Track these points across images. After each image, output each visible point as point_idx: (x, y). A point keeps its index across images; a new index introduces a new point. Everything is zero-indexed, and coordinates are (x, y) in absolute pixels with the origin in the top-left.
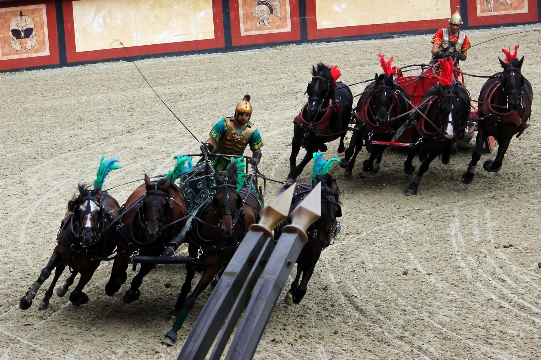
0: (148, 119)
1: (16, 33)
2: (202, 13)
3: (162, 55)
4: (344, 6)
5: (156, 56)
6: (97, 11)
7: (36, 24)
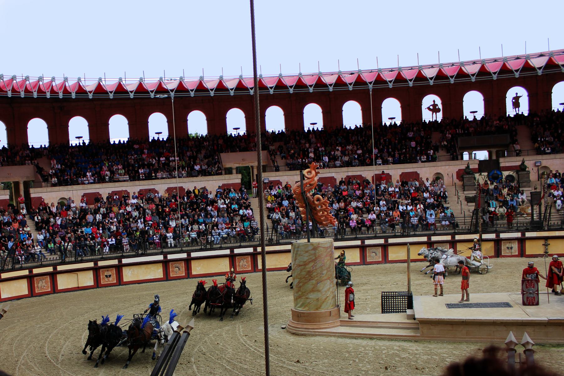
0: (144, 300)
1: (106, 276)
2: (160, 270)
3: (148, 282)
4: (200, 268)
5: (147, 283)
6: (130, 270)
7: (112, 273)
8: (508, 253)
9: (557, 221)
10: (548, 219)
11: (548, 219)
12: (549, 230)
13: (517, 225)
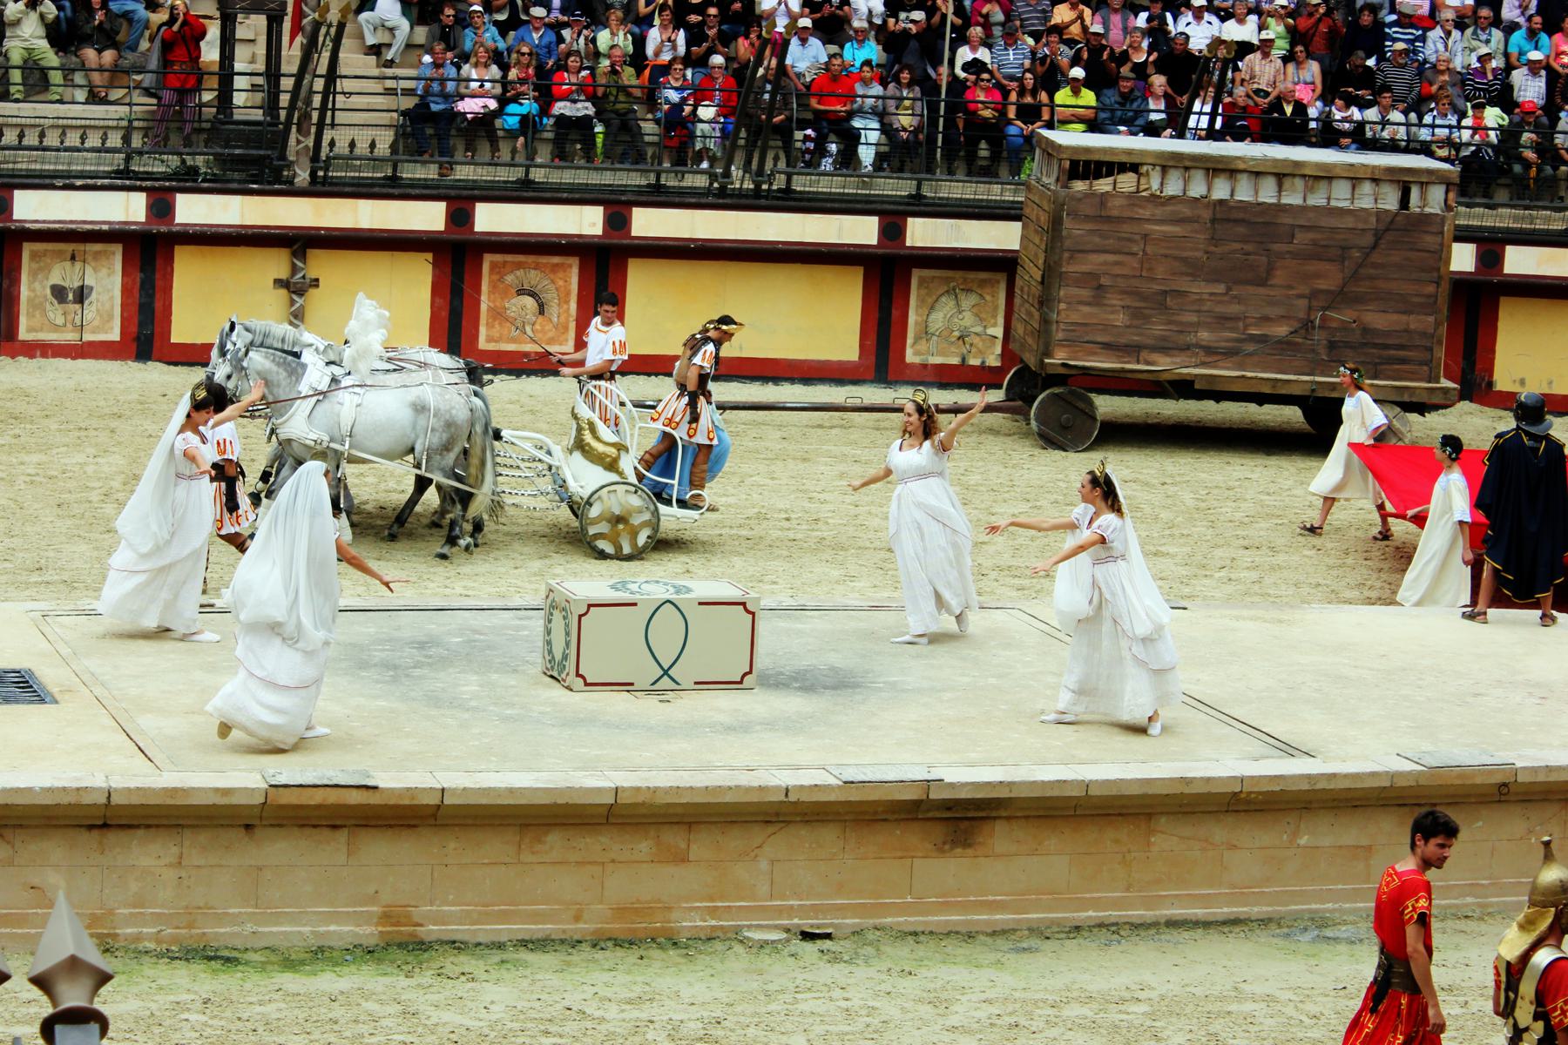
8: (56, 328)
9: (369, 133)
10: (315, 116)
11: (315, 116)
12: (321, 188)
13: (126, 139)
